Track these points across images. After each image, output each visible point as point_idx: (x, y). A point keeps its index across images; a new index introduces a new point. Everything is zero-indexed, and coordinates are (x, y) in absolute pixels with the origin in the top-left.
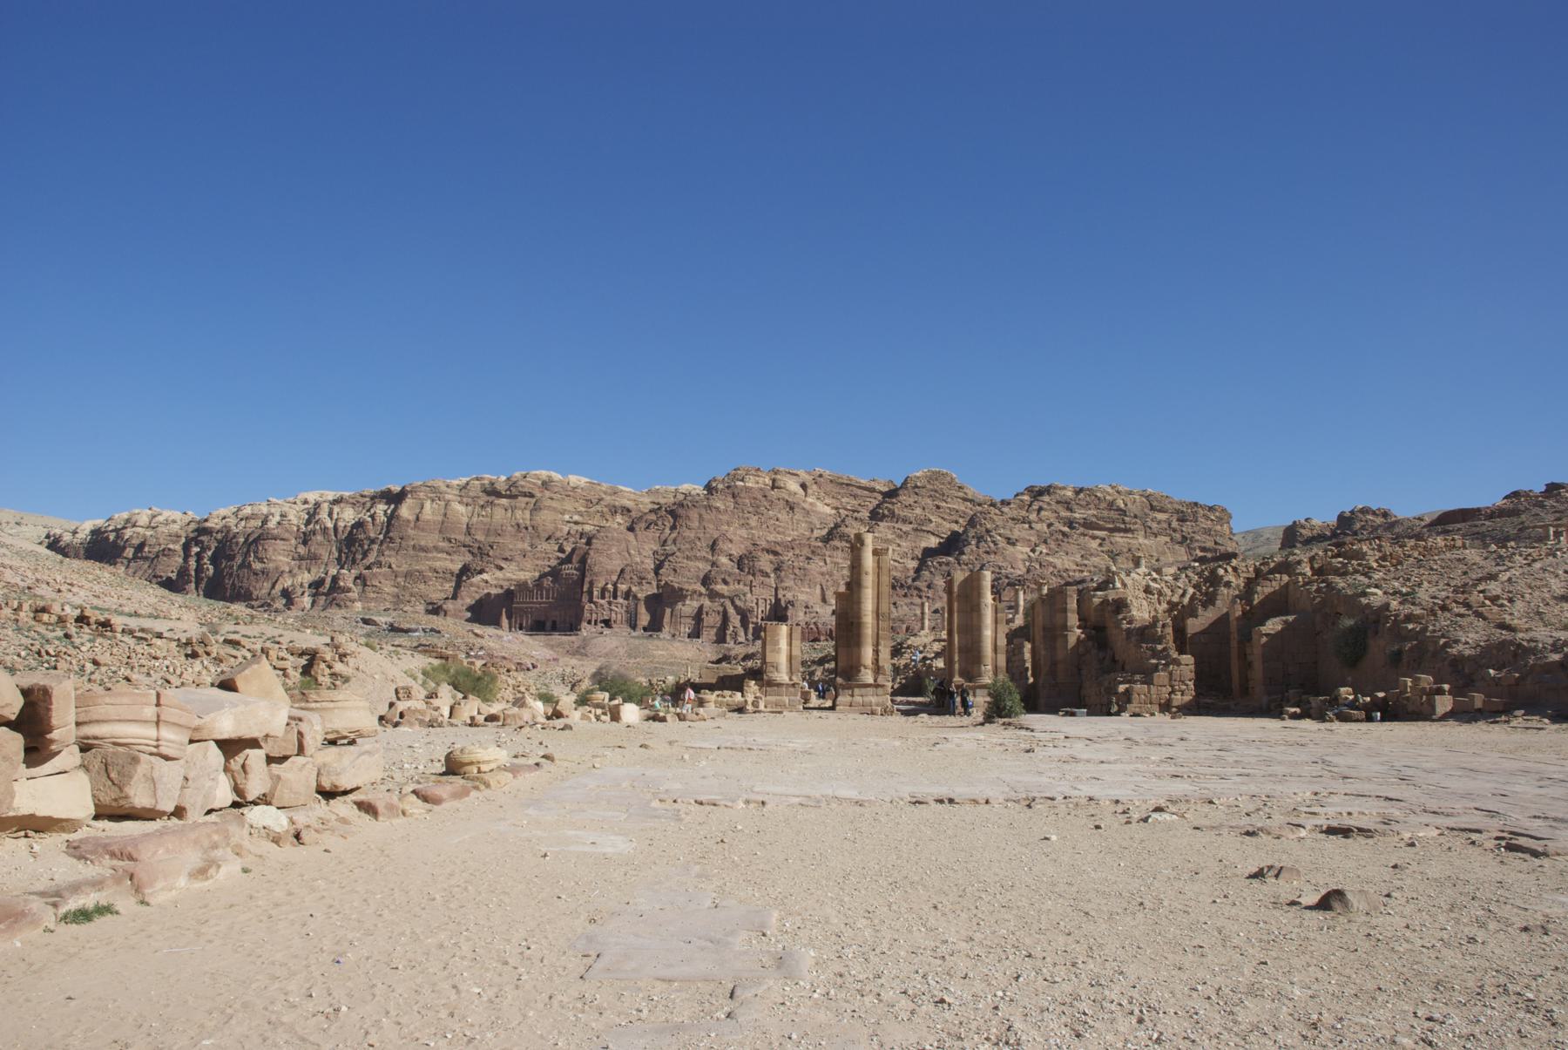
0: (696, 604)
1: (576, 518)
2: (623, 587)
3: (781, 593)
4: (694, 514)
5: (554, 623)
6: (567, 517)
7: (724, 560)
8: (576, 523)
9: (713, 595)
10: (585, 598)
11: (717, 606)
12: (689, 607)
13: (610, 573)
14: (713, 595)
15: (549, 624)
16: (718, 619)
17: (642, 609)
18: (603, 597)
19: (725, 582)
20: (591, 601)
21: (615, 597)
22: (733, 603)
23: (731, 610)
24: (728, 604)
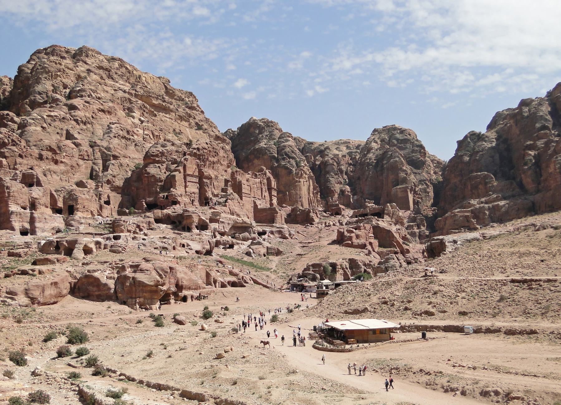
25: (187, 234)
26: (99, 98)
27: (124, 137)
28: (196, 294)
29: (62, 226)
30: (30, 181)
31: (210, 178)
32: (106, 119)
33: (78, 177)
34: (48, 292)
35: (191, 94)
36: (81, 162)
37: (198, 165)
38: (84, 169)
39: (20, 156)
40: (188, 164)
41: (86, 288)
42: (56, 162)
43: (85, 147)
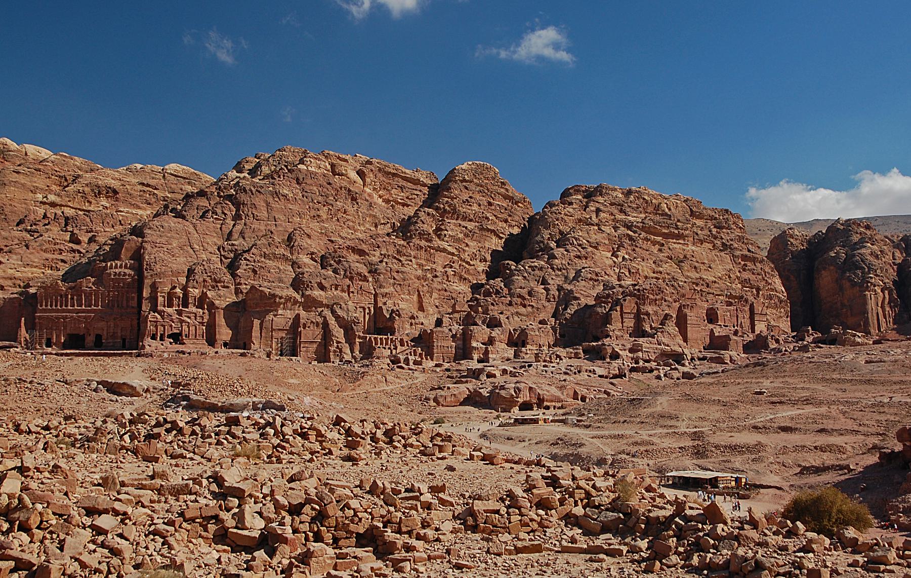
0: (290, 314)
1: (52, 198)
2: (195, 292)
3: (381, 301)
4: (259, 201)
5: (99, 337)
6: (40, 197)
7: (305, 259)
8: (53, 205)
9: (310, 304)
10: (146, 306)
11: (313, 316)
12: (282, 317)
13: (177, 274)
14: (310, 304)
15: (90, 339)
16: (319, 331)
17: (221, 320)
18: (170, 305)
19: (322, 287)
20: (154, 309)
21: (186, 305)
22: (333, 312)
23: (332, 321)
24: (327, 313)
25: (600, 362)
26: (580, 245)
27: (591, 279)
28: (560, 405)
29: (512, 356)
30: (493, 324)
31: (648, 314)
32: (581, 263)
33: (542, 316)
34: (449, 399)
35: (727, 211)
36: (547, 304)
37: (636, 303)
38: (551, 307)
39: (492, 304)
40: (625, 304)
41: (474, 400)
42: (525, 306)
43: (554, 292)
